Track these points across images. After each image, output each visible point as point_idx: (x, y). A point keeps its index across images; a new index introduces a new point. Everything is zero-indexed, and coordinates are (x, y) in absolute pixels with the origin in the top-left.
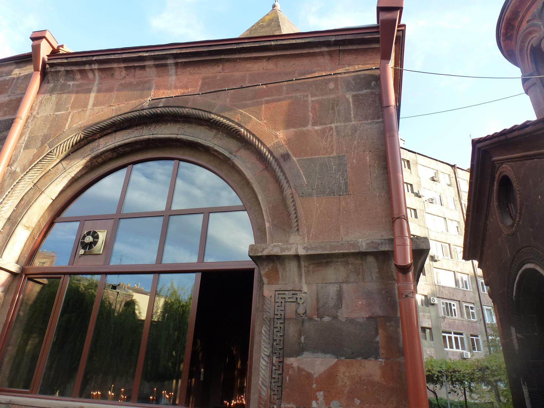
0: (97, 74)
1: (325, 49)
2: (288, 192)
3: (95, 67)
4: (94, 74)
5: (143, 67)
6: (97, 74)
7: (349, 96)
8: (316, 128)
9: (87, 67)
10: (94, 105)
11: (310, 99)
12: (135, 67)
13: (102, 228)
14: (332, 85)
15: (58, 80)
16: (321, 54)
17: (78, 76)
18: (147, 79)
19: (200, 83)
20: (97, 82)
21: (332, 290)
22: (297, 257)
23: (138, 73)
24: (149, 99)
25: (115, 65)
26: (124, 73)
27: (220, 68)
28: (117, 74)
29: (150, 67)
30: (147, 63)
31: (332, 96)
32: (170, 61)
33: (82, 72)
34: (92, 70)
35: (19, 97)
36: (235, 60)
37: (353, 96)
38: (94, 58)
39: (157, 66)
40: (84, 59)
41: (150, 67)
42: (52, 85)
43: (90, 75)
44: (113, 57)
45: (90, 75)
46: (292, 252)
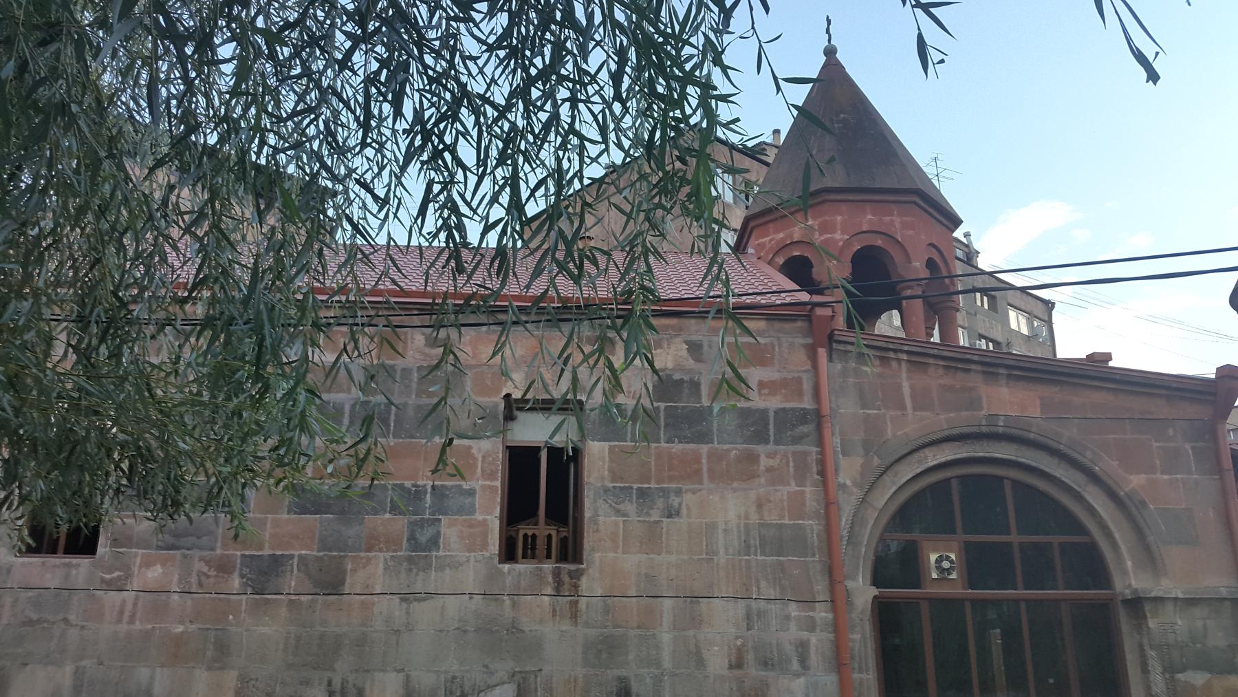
0: (904, 364)
1: (1164, 392)
2: (1151, 538)
3: (905, 357)
4: (900, 364)
5: (967, 371)
6: (904, 364)
7: (1188, 446)
8: (1166, 477)
9: (892, 355)
10: (915, 409)
11: (1156, 445)
12: (957, 368)
13: (951, 551)
14: (1171, 432)
15: (847, 362)
16: (1160, 396)
17: (877, 362)
18: (971, 385)
19: (1038, 402)
20: (904, 375)
21: (1199, 623)
22: (1176, 599)
23: (960, 375)
24: (984, 412)
25: (931, 361)
26: (941, 371)
27: (1057, 389)
28: (931, 370)
29: (976, 371)
30: (973, 367)
31: (1173, 444)
32: (1002, 371)
33: (882, 358)
34: (899, 360)
35: (796, 375)
36: (1074, 384)
37: (1193, 448)
38: (906, 348)
39: (984, 373)
40: (891, 346)
41: (976, 371)
42: (839, 366)
43: (894, 364)
44: (932, 352)
45: (894, 364)
46: (1173, 596)
